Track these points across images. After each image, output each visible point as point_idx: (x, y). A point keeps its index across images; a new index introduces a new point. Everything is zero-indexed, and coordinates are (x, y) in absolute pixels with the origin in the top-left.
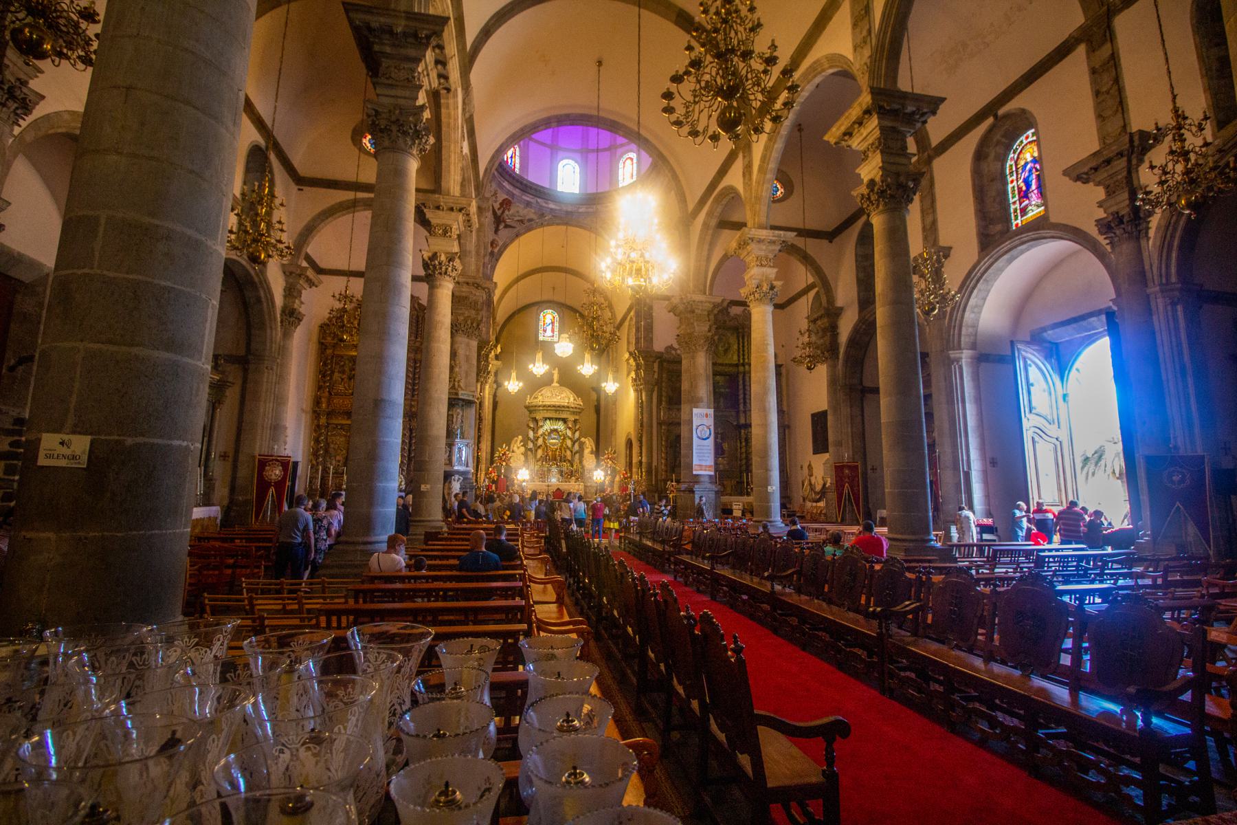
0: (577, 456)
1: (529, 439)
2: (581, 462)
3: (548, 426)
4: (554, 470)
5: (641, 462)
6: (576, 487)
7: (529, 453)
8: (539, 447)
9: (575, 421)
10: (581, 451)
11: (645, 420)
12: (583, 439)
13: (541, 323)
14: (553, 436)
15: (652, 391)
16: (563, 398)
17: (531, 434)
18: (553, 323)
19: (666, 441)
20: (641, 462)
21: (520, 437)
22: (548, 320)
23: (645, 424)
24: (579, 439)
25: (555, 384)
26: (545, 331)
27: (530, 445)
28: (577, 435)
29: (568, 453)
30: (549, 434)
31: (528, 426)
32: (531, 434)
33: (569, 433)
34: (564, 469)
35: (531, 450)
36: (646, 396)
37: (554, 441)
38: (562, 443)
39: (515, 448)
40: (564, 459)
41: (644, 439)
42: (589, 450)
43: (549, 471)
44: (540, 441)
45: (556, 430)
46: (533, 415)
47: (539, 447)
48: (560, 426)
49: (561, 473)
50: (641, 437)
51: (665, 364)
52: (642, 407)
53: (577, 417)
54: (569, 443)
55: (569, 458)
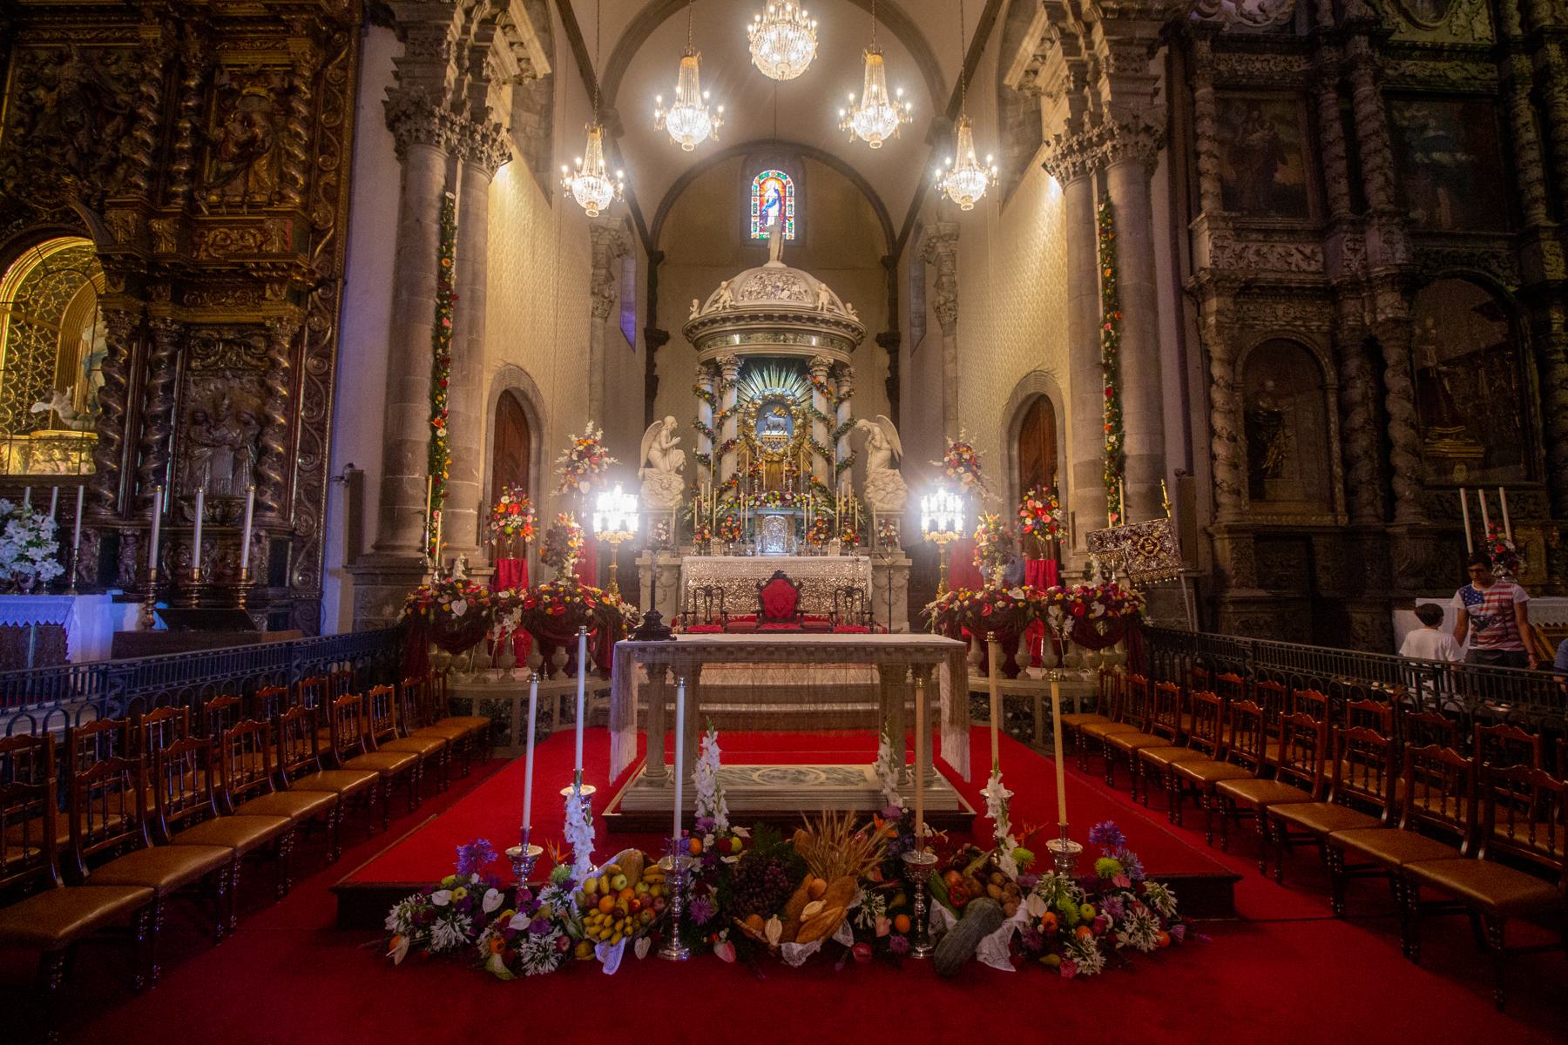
0: (847, 474)
1: (700, 427)
2: (859, 491)
3: (759, 387)
4: (775, 514)
5: (1117, 461)
6: (847, 570)
7: (701, 469)
8: (727, 447)
9: (835, 371)
10: (856, 462)
11: (1128, 278)
12: (862, 423)
13: (755, 201)
14: (772, 419)
15: (1150, 169)
16: (798, 296)
17: (705, 413)
18: (781, 200)
19: (1230, 363)
20: (1117, 461)
21: (670, 420)
22: (771, 195)
23: (1129, 300)
24: (849, 425)
25: (774, 264)
26: (764, 217)
27: (705, 447)
28: (845, 411)
29: (819, 463)
30: (761, 412)
31: (697, 389)
32: (705, 413)
33: (820, 403)
34: (807, 514)
35: (704, 459)
36: (1129, 181)
37: (775, 435)
38: (802, 436)
39: (655, 455)
40: (800, 482)
41: (1128, 361)
42: (883, 455)
43: (757, 520)
44: (731, 430)
45: (779, 401)
46: (706, 355)
47: (727, 447)
48: (790, 387)
49: (797, 526)
50: (1114, 353)
51: (1203, 48)
52: (1109, 230)
53: (843, 356)
54: (819, 433)
55: (822, 479)
